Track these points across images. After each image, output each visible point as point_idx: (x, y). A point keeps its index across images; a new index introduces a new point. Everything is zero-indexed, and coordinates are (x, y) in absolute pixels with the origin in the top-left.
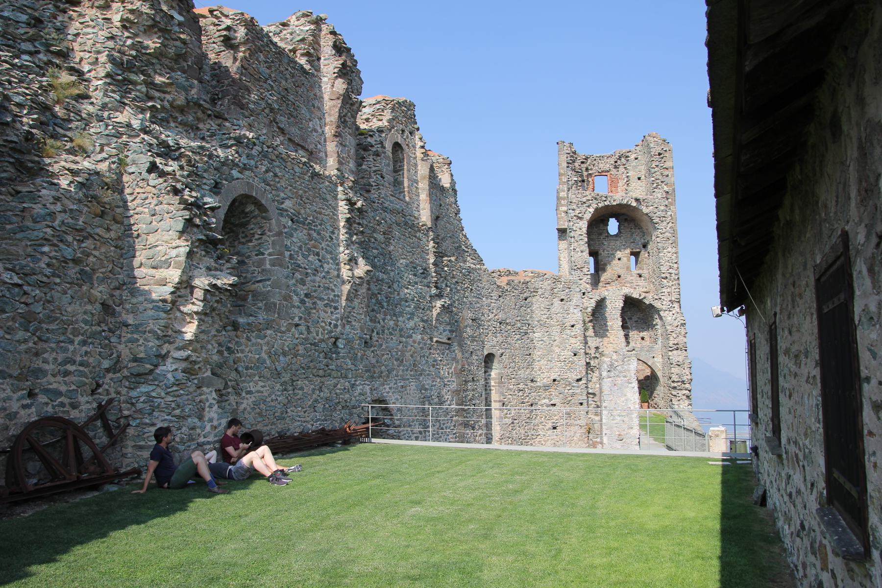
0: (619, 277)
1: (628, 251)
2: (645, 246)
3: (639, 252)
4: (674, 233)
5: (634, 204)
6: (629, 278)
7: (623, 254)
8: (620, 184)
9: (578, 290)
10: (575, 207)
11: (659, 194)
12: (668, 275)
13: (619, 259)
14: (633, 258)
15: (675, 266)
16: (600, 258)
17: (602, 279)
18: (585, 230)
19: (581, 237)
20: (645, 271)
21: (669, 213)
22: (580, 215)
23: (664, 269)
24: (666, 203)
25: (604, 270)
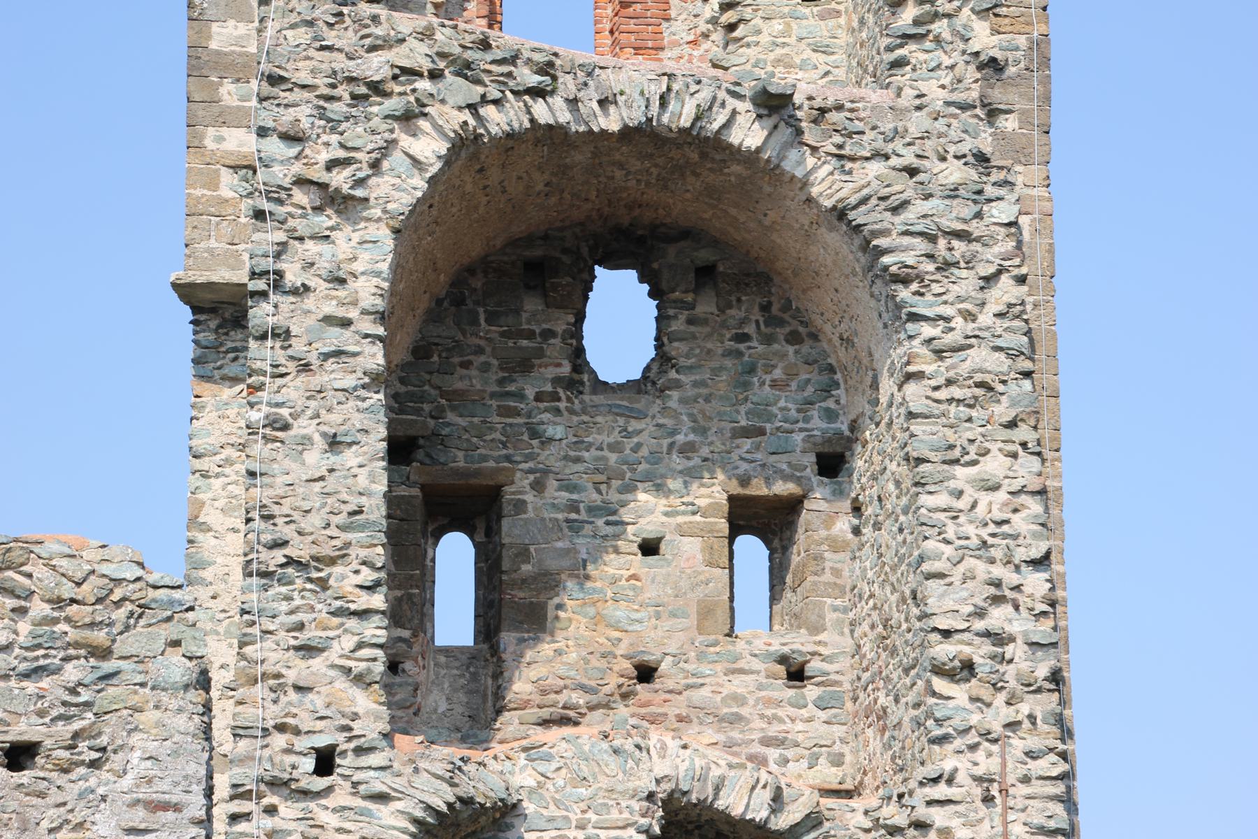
0: (646, 673)
1: (713, 493)
2: (832, 464)
3: (791, 507)
4: (1030, 356)
5: (749, 134)
6: (717, 687)
7: (680, 510)
8: (678, 29)
9: (176, 668)
10: (303, 115)
11: (935, 77)
12: (980, 652)
13: (650, 548)
14: (751, 549)
15: (1036, 583)
16: (510, 531)
17: (521, 687)
18: (369, 290)
19: (335, 338)
20: (834, 641)
21: (1001, 212)
22: (340, 180)
23: (947, 603)
24: (985, 141)
25: (536, 621)
